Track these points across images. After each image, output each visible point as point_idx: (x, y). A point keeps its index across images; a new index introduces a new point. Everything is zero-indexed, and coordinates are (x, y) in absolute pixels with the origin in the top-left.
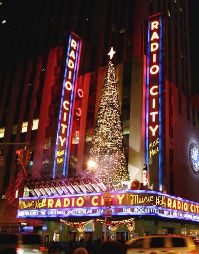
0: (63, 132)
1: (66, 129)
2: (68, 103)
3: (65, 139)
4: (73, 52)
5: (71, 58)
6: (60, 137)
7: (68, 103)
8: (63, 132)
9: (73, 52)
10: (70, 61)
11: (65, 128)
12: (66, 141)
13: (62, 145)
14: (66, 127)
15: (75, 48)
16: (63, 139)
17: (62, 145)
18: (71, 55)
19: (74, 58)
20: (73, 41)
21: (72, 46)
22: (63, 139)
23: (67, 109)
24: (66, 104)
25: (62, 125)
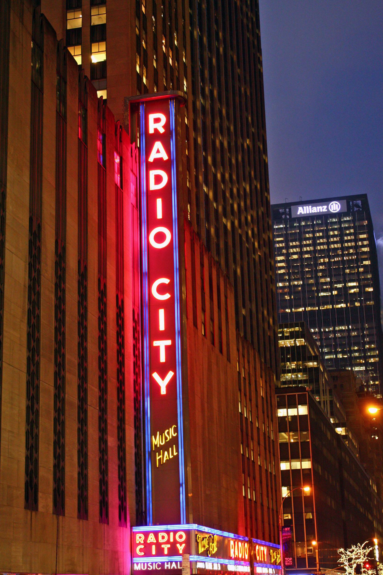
0: (163, 359)
1: (170, 350)
2: (166, 281)
3: (170, 375)
4: (158, 145)
5: (158, 164)
6: (155, 376)
7: (166, 281)
8: (163, 359)
9: (158, 145)
10: (153, 173)
11: (167, 347)
12: (174, 380)
13: (163, 391)
14: (169, 342)
15: (162, 131)
16: (163, 377)
17: (163, 391)
18: (151, 159)
19: (166, 158)
20: (152, 117)
21: (151, 131)
22: (163, 377)
23: (167, 296)
24: (162, 289)
25: (156, 343)
